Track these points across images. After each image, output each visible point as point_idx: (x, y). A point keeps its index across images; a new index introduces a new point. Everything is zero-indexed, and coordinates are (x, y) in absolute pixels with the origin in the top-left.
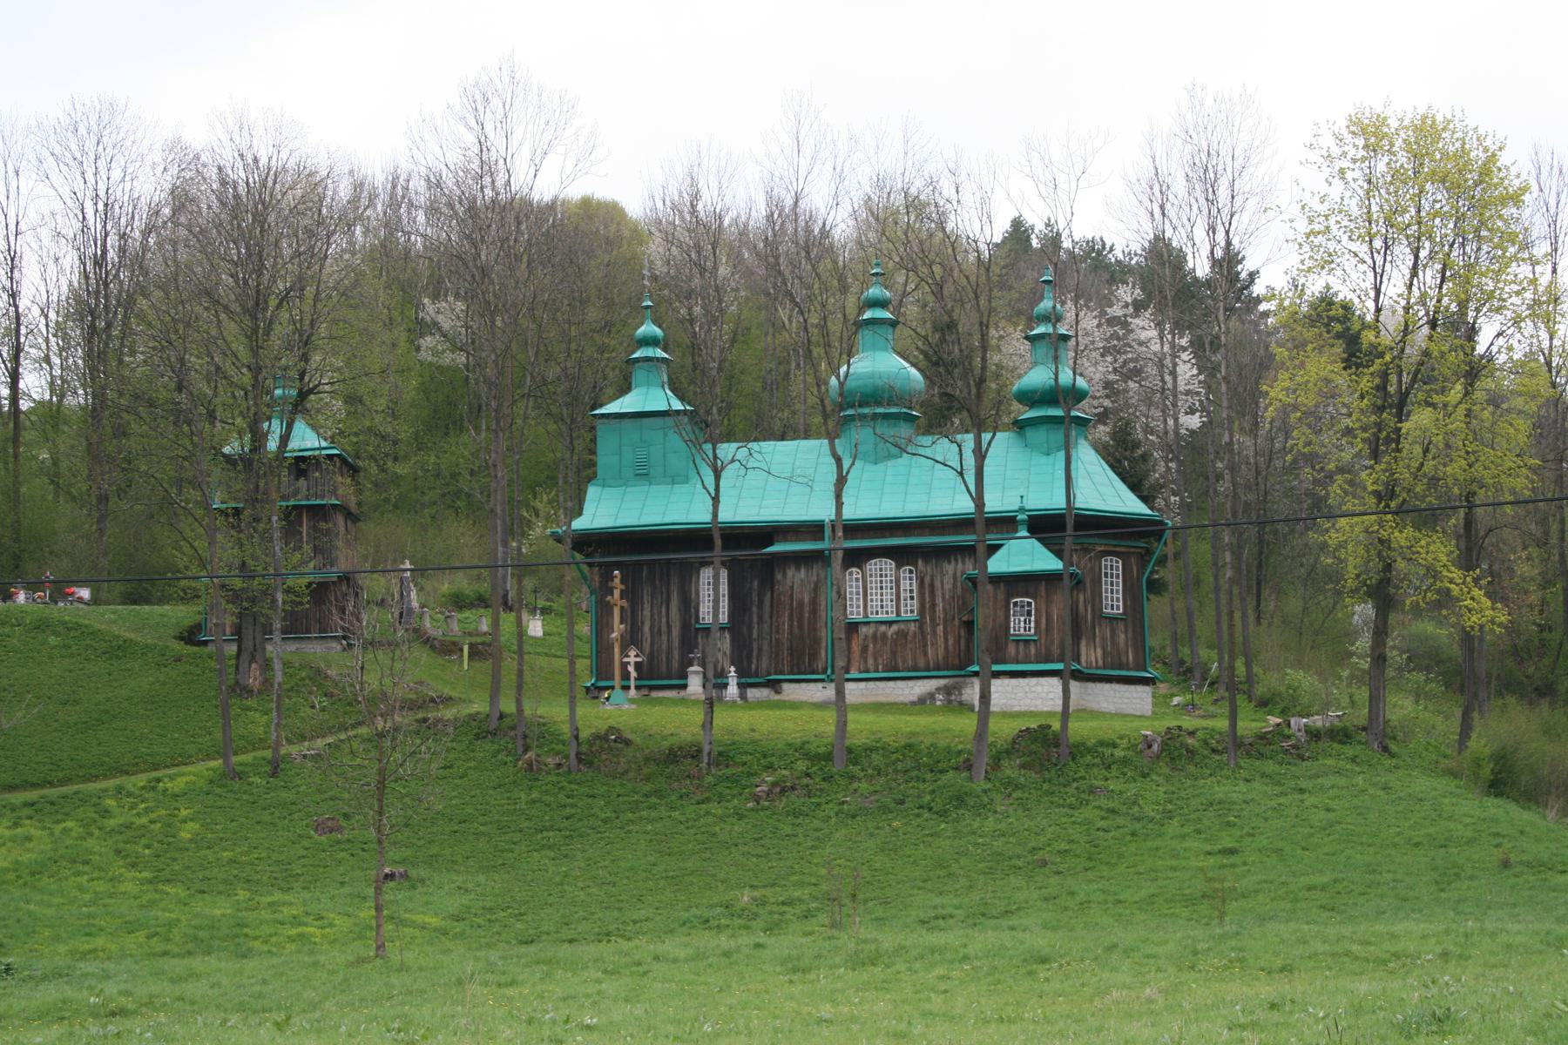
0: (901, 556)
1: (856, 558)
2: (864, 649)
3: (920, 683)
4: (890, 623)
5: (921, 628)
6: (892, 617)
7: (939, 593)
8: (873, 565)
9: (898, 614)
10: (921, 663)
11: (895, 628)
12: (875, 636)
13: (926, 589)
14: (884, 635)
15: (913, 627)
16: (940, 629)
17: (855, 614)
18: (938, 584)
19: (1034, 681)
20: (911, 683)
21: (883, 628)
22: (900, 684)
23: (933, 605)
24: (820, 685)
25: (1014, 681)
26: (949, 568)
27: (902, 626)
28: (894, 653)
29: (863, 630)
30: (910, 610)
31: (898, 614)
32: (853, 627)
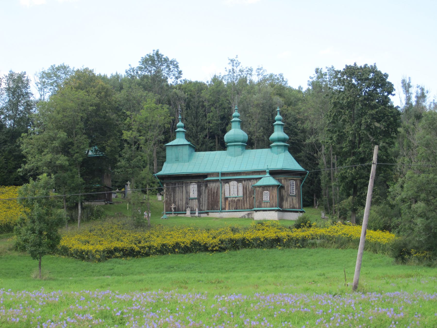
0: (239, 181)
2: (229, 204)
3: (243, 212)
5: (243, 198)
6: (236, 196)
8: (232, 183)
9: (238, 195)
10: (243, 207)
11: (237, 198)
12: (232, 201)
13: (245, 189)
15: (241, 198)
17: (227, 195)
18: (247, 187)
20: (241, 213)
21: (234, 199)
25: (264, 212)
26: (250, 183)
27: (239, 198)
28: (237, 205)
29: (229, 199)
30: (241, 194)
31: (238, 195)
32: (226, 199)
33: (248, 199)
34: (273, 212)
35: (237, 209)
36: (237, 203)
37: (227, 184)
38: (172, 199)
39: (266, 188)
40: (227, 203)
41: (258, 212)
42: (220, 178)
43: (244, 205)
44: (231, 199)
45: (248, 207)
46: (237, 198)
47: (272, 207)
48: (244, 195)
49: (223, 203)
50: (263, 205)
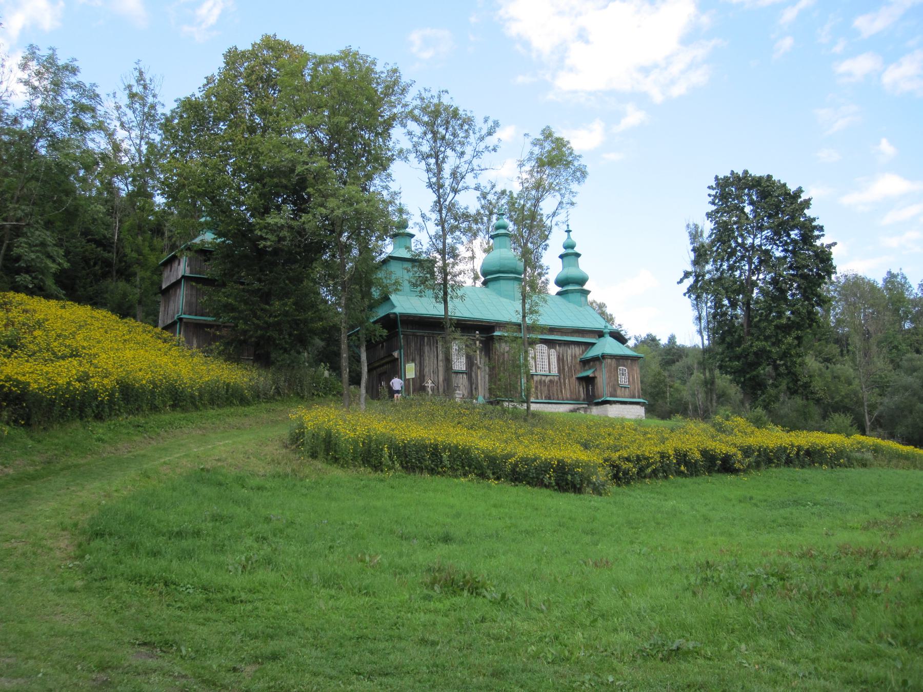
0: (550, 343)
2: (536, 388)
6: (547, 373)
12: (540, 381)
13: (560, 360)
15: (556, 378)
17: (533, 372)
19: (631, 406)
20: (558, 406)
21: (543, 378)
22: (554, 406)
23: (564, 369)
25: (623, 406)
26: (569, 352)
30: (555, 371)
33: (567, 381)
34: (638, 407)
35: (550, 399)
36: (548, 386)
41: (614, 406)
46: (548, 379)
47: (634, 397)
50: (619, 392)
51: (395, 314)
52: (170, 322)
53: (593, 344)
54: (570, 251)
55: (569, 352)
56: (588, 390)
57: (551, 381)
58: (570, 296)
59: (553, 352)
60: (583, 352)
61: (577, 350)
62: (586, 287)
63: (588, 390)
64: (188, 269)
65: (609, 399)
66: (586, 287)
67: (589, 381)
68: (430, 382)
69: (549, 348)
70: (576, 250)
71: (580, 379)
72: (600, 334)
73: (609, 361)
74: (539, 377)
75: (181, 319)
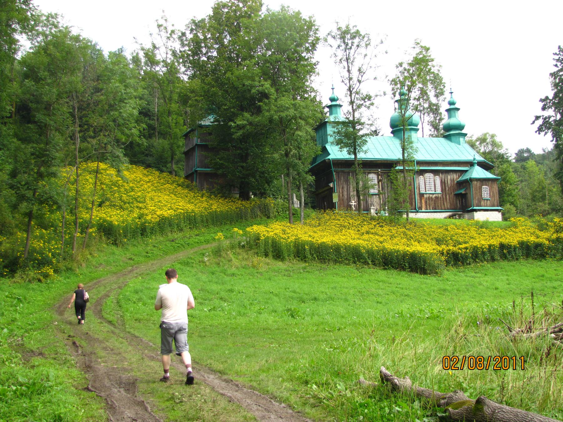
1: (422, 172)
2: (426, 202)
3: (444, 213)
4: (433, 194)
6: (433, 192)
7: (447, 185)
8: (427, 175)
11: (434, 195)
13: (443, 183)
14: (432, 198)
16: (448, 196)
17: (423, 191)
18: (446, 182)
21: (431, 196)
24: (414, 214)
27: (437, 195)
28: (435, 204)
29: (425, 196)
30: (439, 191)
32: (421, 195)
33: (448, 196)
34: (497, 212)
35: (436, 209)
36: (434, 201)
37: (421, 176)
38: (345, 193)
39: (484, 182)
40: (423, 201)
41: (478, 212)
42: (417, 168)
43: (444, 204)
44: (428, 195)
45: (449, 207)
48: (442, 191)
49: (419, 201)
50: (482, 203)
51: (329, 159)
52: (190, 172)
53: (466, 171)
54: (452, 107)
55: (449, 177)
56: (462, 202)
57: (436, 197)
58: (453, 138)
59: (438, 179)
60: (459, 177)
61: (455, 176)
62: (463, 131)
63: (462, 202)
64: (199, 140)
65: (475, 208)
66: (463, 131)
67: (463, 197)
68: (353, 201)
69: (435, 175)
70: (456, 106)
71: (457, 195)
72: (471, 164)
73: (475, 182)
74: (428, 195)
75: (196, 171)
